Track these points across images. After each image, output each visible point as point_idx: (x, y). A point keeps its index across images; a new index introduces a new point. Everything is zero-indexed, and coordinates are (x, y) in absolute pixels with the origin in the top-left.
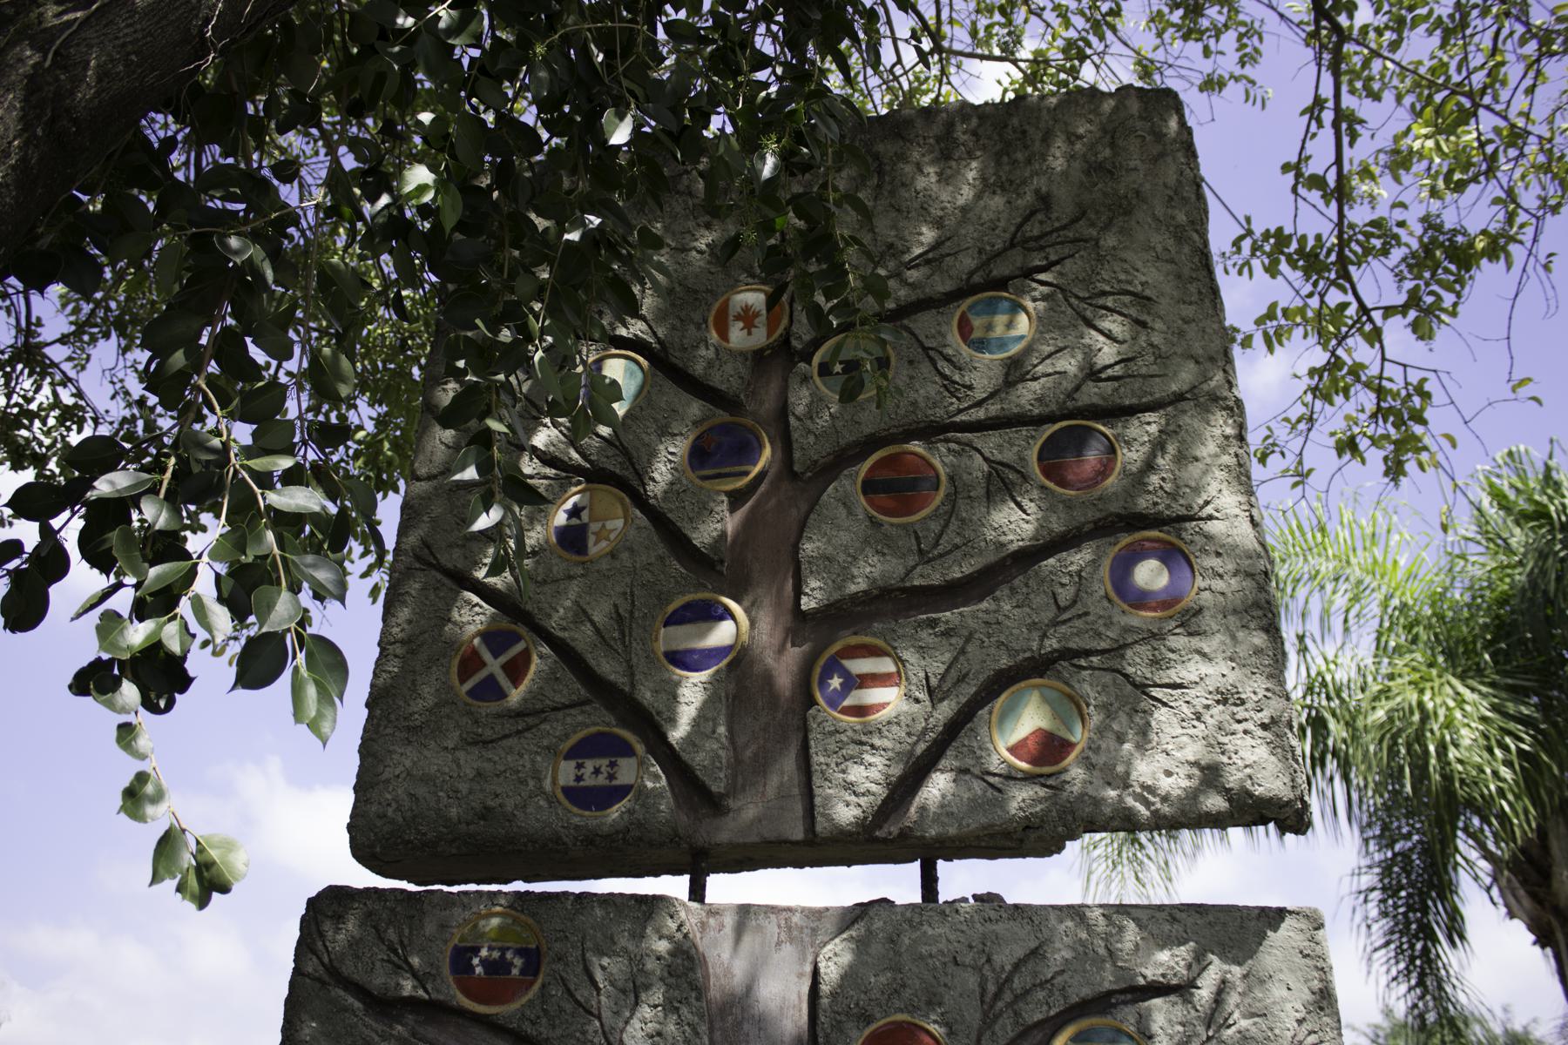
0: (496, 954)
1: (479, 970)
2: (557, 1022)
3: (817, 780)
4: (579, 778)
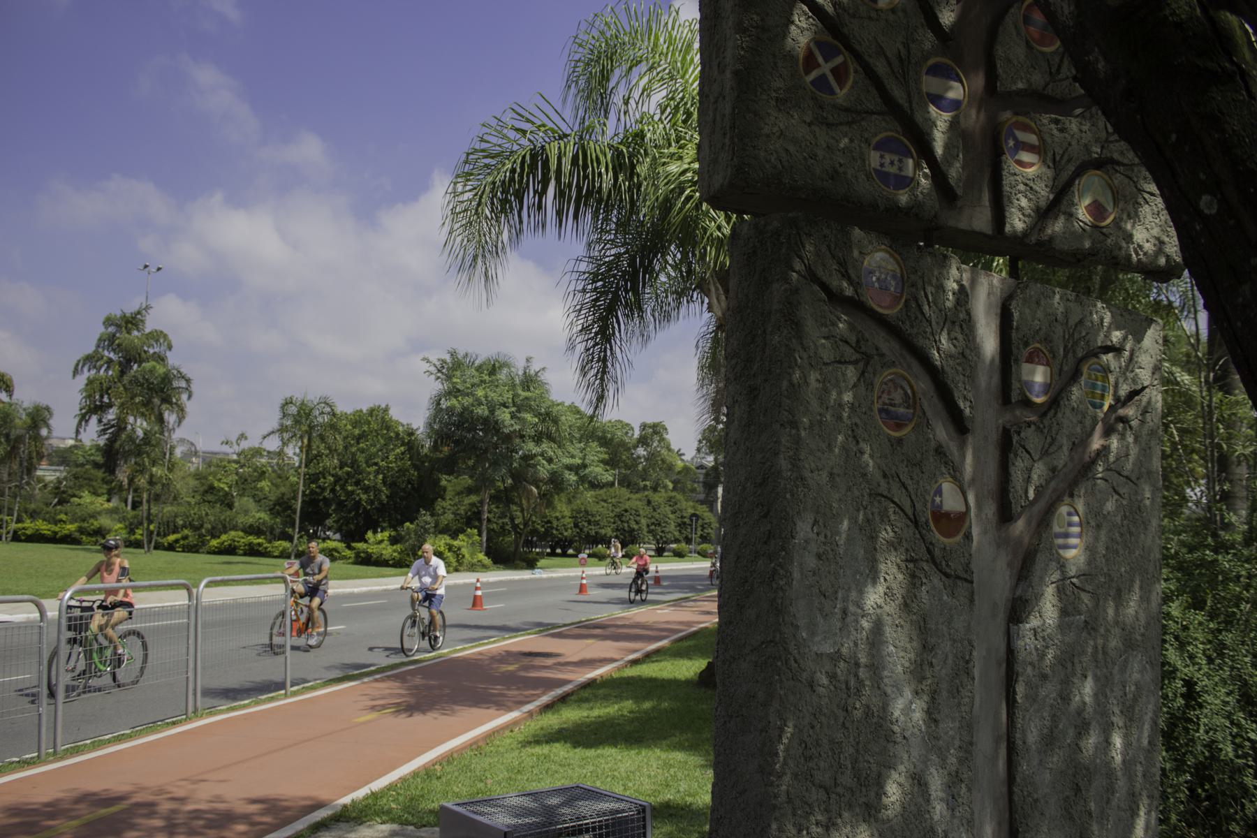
4: (882, 165)
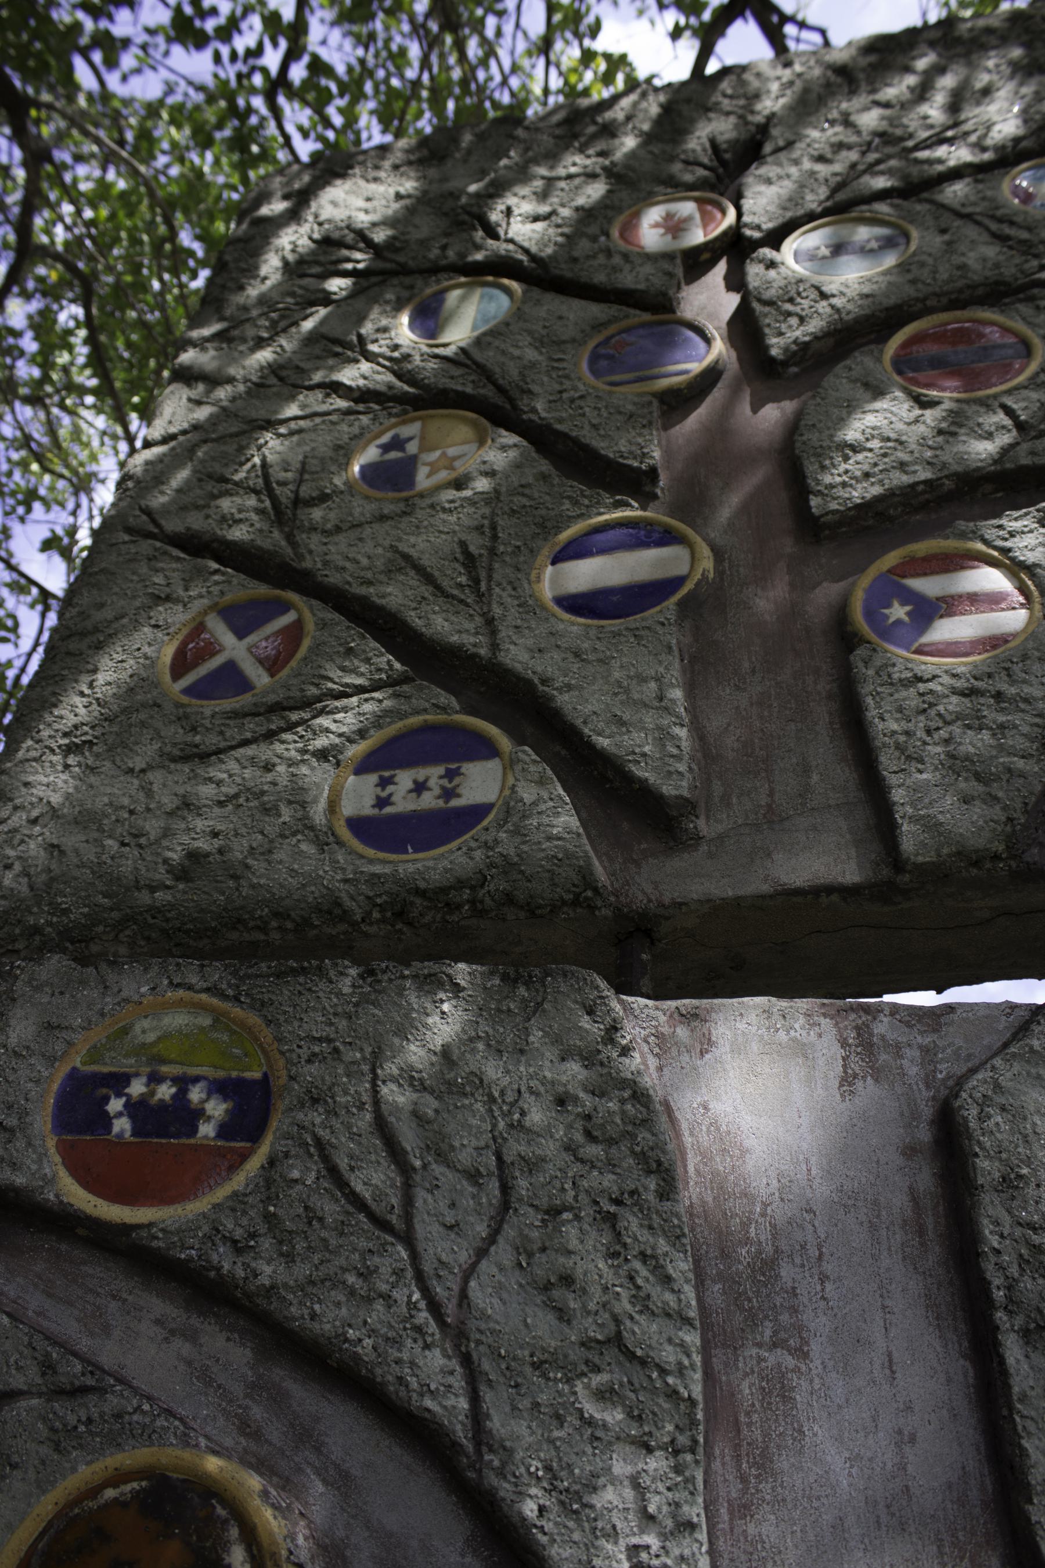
0: (165, 1092)
1: (122, 1125)
2: (300, 1246)
3: (888, 762)
4: (382, 802)
